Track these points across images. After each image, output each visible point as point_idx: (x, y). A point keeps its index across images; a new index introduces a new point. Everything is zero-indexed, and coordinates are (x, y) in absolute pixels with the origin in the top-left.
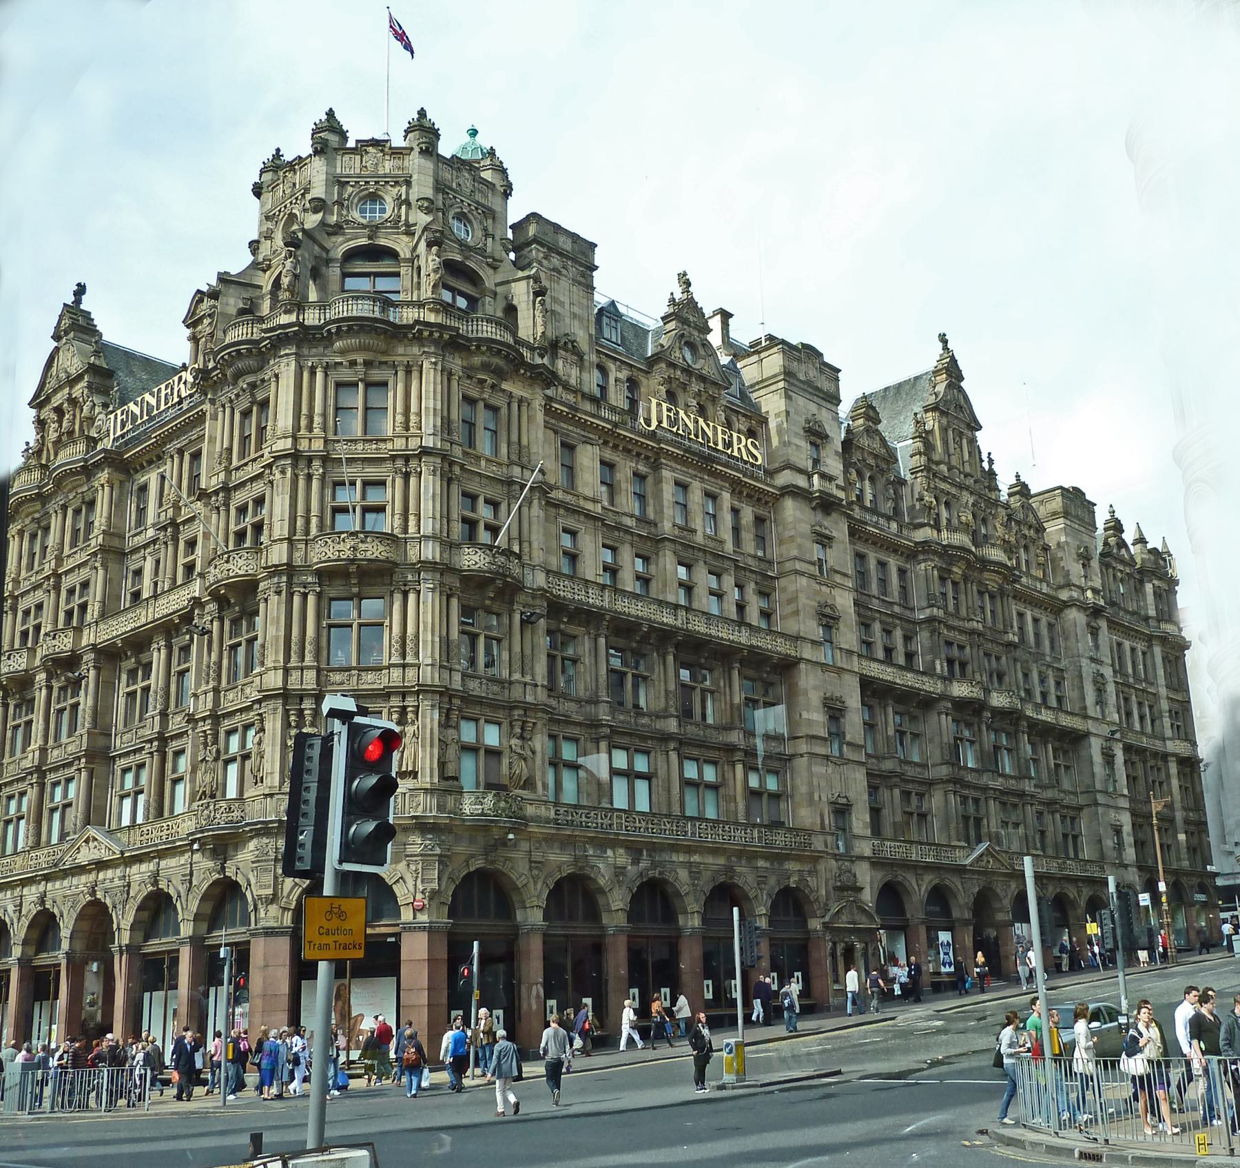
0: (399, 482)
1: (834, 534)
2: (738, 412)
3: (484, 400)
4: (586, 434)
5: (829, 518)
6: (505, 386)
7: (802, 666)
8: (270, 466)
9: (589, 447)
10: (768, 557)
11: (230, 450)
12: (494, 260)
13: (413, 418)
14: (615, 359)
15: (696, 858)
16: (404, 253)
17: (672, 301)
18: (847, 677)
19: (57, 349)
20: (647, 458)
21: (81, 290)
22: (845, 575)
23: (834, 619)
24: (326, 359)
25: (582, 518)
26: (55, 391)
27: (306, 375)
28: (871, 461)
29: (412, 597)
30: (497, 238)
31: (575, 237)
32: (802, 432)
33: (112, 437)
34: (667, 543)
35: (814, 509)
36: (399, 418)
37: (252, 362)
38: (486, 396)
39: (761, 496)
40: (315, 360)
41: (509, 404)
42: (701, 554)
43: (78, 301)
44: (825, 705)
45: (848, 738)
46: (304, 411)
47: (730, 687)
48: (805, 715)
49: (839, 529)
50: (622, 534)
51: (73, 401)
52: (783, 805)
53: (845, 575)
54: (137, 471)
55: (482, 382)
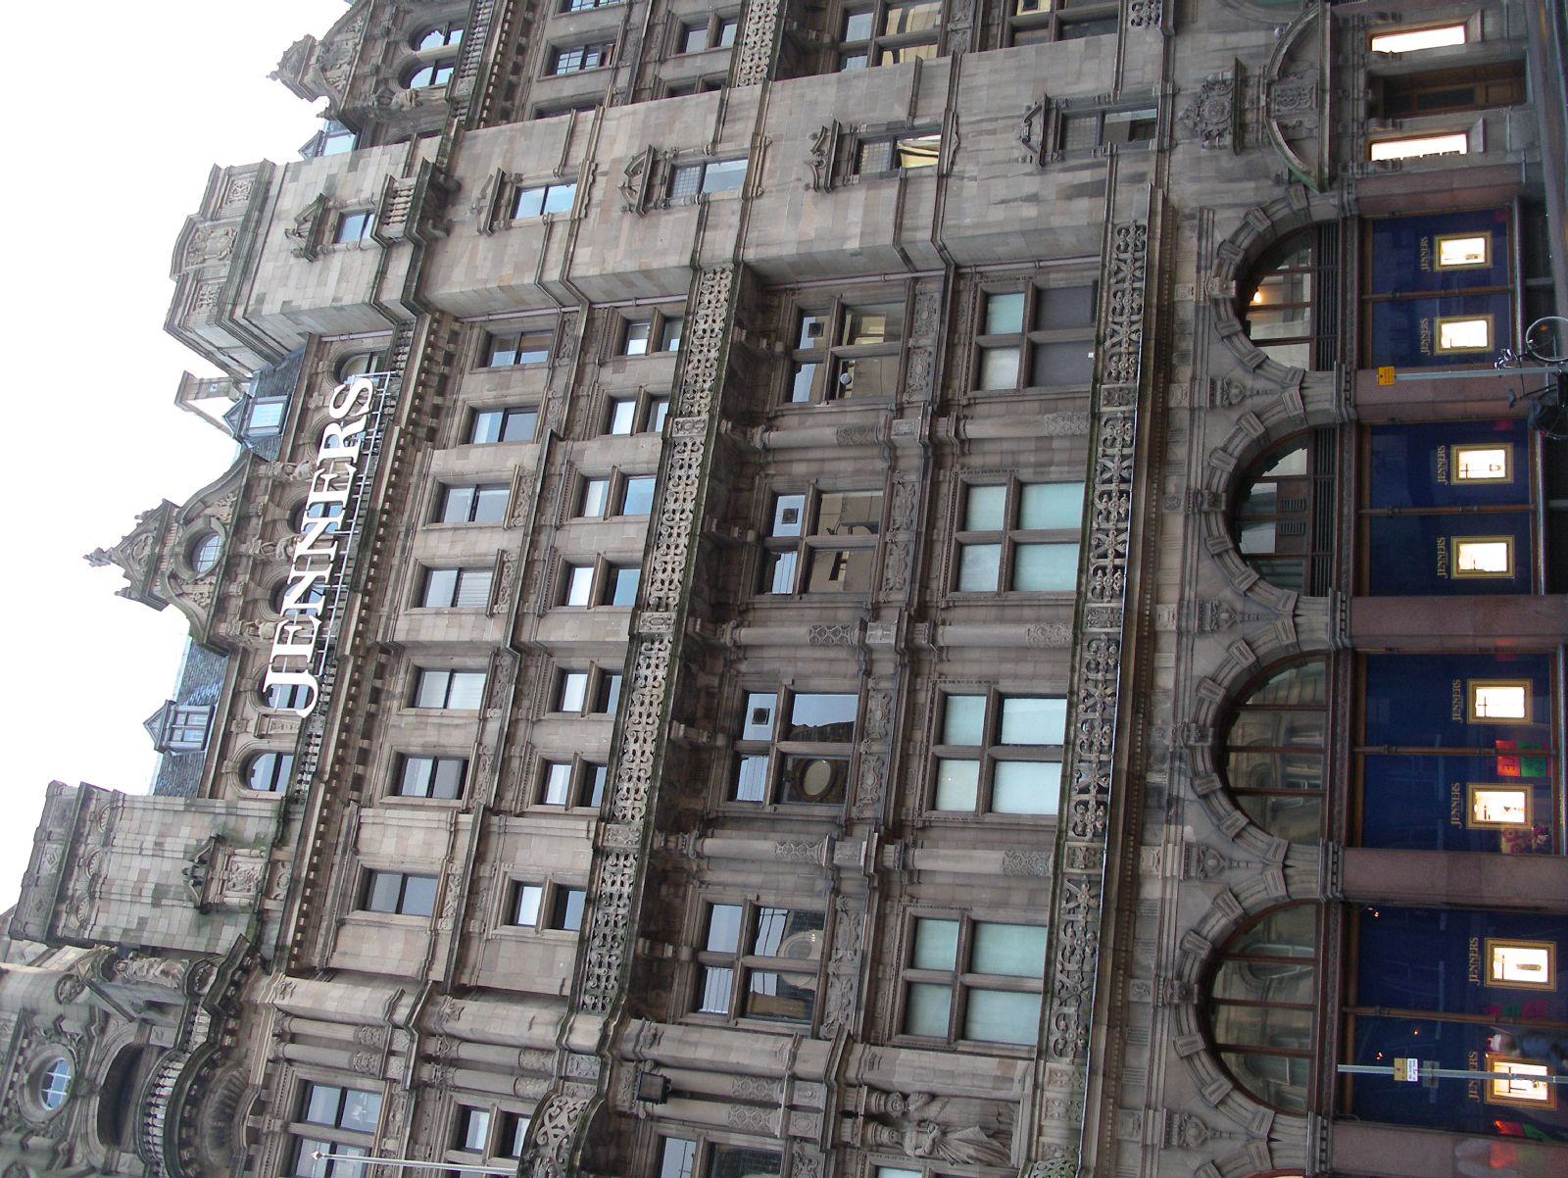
1: (493, 171)
2: (305, 410)
3: (285, 1127)
4: (340, 848)
5: (467, 184)
6: (259, 1080)
7: (750, 255)
9: (365, 833)
10: (554, 323)
12: (92, 1021)
14: (227, 735)
15: (1167, 617)
17: (126, 593)
18: (774, 120)
20: (381, 672)
22: (572, 133)
23: (655, 163)
25: (485, 871)
28: (377, 55)
30: (60, 1009)
31: (42, 836)
32: (318, 265)
34: (525, 637)
35: (448, 231)
38: (277, 1125)
39: (440, 356)
41: (290, 1061)
42: (543, 538)
44: (831, 188)
45: (900, 113)
47: (806, 448)
48: (853, 245)
49: (491, 151)
50: (516, 751)
52: (1056, 280)
53: (572, 133)
55: (255, 1136)
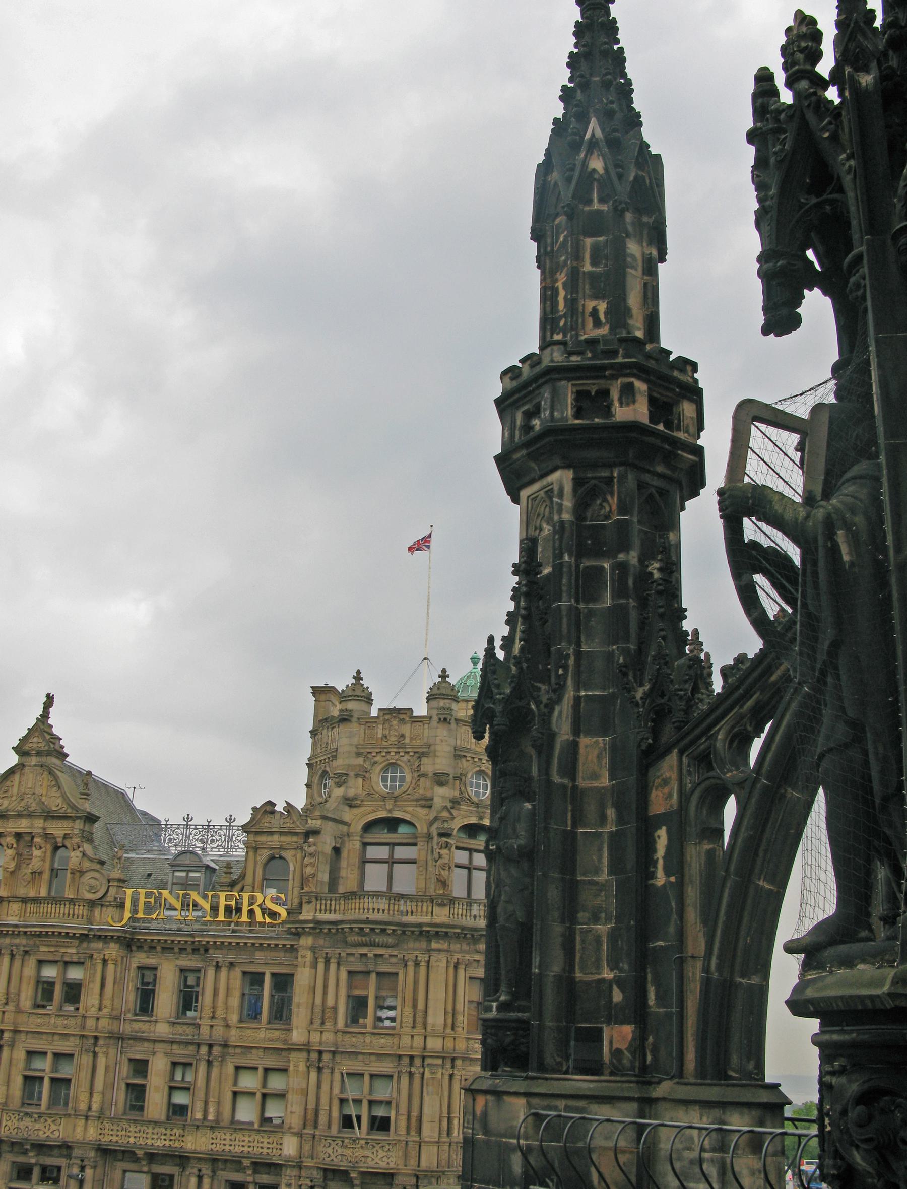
8: (412, 1058)
11: (335, 1009)
19: (20, 767)
21: (50, 700)
24: (468, 957)
26: (20, 816)
27: (451, 970)
33: (127, 915)
37: (390, 940)
40: (458, 956)
43: (45, 715)
46: (450, 1009)
51: (46, 836)
54: (140, 948)
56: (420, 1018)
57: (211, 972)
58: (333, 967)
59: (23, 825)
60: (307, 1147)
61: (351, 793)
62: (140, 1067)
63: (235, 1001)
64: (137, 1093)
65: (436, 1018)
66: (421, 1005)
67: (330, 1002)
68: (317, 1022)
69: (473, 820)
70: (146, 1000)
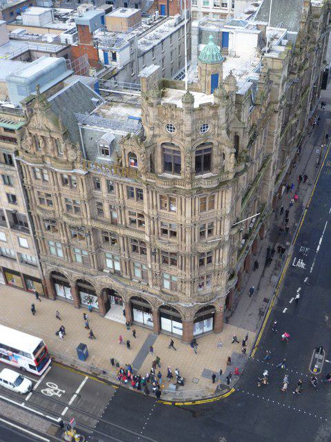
0: (219, 223)
13: (223, 206)
16: (215, 143)
27: (193, 200)
29: (221, 250)
36: (220, 206)
51: (51, 138)
56: (183, 213)
57: (116, 186)
58: (154, 194)
59: (43, 134)
60: (152, 240)
61: (156, 132)
62: (100, 204)
63: (125, 193)
64: (101, 212)
65: (188, 214)
66: (183, 210)
67: (155, 204)
68: (151, 208)
69: (202, 142)
70: (98, 186)
